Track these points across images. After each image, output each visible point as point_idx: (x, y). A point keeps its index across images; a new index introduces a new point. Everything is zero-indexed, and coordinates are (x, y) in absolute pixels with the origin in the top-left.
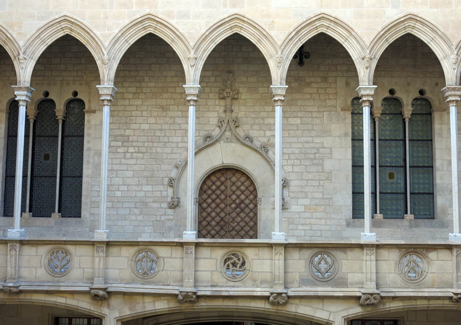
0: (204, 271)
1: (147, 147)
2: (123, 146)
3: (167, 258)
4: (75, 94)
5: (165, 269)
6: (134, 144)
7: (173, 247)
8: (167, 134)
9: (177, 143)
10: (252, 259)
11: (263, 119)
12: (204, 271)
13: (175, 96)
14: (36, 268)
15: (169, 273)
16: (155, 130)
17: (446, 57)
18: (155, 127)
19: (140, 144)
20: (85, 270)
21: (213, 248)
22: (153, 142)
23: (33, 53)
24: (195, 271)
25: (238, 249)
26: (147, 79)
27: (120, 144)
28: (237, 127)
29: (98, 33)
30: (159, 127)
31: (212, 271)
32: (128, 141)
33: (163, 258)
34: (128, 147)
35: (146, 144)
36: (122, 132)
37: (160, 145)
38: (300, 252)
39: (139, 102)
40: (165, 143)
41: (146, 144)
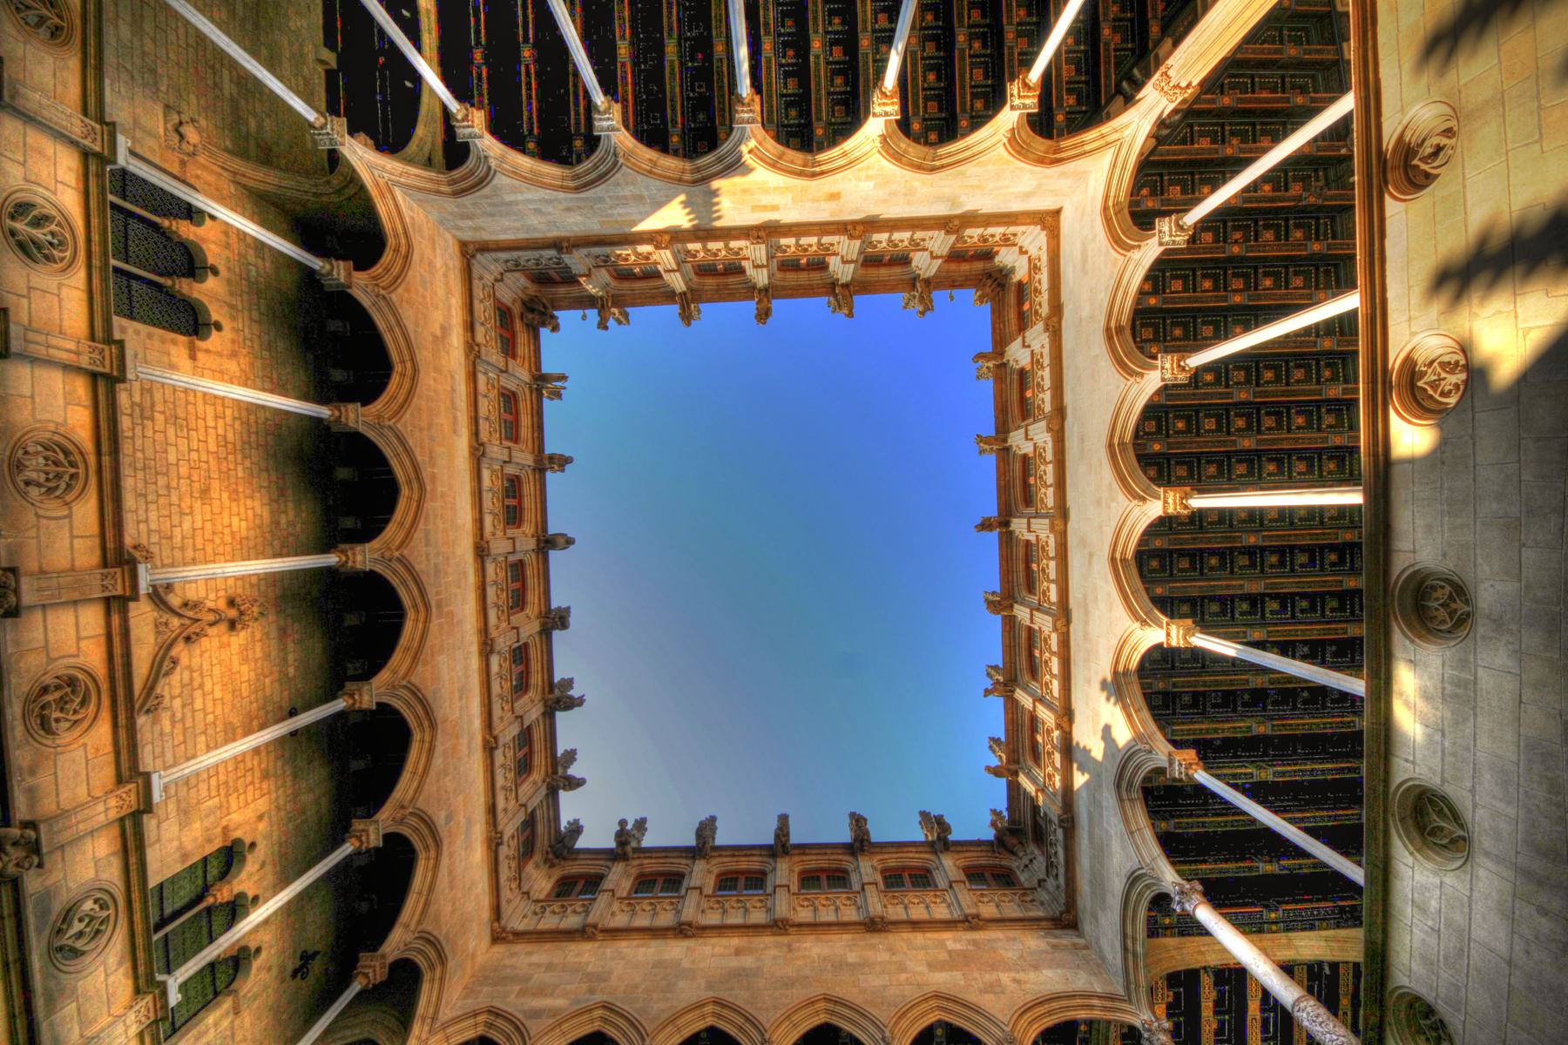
0: (45, 627)
1: (134, 456)
2: (133, 404)
3: (71, 528)
4: (218, 327)
5: (44, 521)
6: (138, 429)
7: (97, 541)
8: (162, 500)
9: (146, 521)
10: (85, 745)
11: (201, 686)
12: (45, 627)
13: (226, 514)
14: (24, 164)
15: (33, 533)
16: (166, 474)
17: (406, 926)
18: (173, 474)
19: (139, 442)
20: (25, 302)
21: (103, 640)
22: (144, 469)
23: (380, 310)
24: (44, 606)
25: (106, 702)
26: (247, 463)
27: (137, 399)
28: (188, 639)
29: (408, 416)
30: (174, 484)
31: (46, 647)
32: (143, 417)
33: (69, 516)
34: (131, 415)
35: (139, 455)
36: (159, 408)
37: (140, 485)
38: (113, 854)
39: (212, 447)
40: (145, 496)
41: (139, 455)
